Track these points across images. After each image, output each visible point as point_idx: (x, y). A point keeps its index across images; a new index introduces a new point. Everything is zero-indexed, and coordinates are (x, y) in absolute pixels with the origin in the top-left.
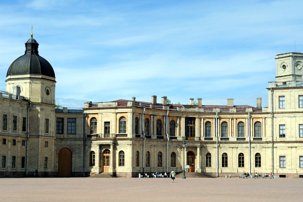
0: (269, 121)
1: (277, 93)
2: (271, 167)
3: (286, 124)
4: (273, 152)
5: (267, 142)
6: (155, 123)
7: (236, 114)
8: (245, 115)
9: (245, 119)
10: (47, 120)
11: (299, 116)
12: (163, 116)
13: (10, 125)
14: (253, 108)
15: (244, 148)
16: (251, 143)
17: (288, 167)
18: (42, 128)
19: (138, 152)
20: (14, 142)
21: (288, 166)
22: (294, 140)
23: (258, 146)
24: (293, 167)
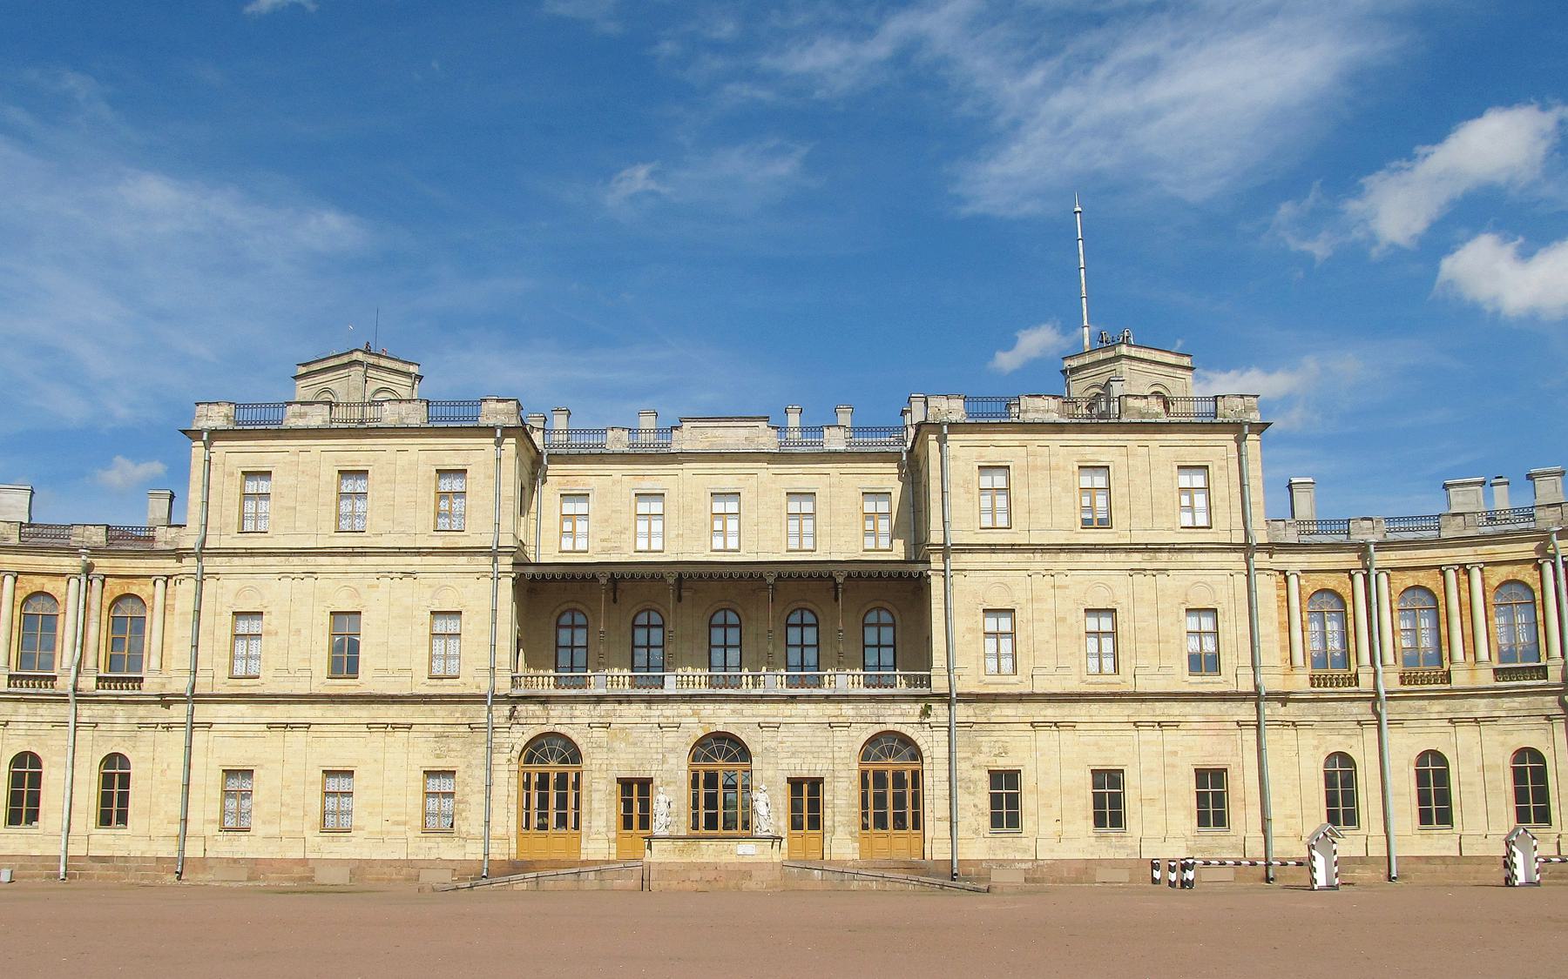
0: (184, 592)
1: (233, 457)
3: (265, 611)
5: (165, 701)
7: (16, 550)
8: (67, 561)
9: (61, 583)
11: (331, 569)
14: (108, 527)
15: (45, 726)
16: (81, 698)
17: (256, 825)
21: (264, 823)
22: (302, 689)
23: (118, 720)
24: (286, 825)
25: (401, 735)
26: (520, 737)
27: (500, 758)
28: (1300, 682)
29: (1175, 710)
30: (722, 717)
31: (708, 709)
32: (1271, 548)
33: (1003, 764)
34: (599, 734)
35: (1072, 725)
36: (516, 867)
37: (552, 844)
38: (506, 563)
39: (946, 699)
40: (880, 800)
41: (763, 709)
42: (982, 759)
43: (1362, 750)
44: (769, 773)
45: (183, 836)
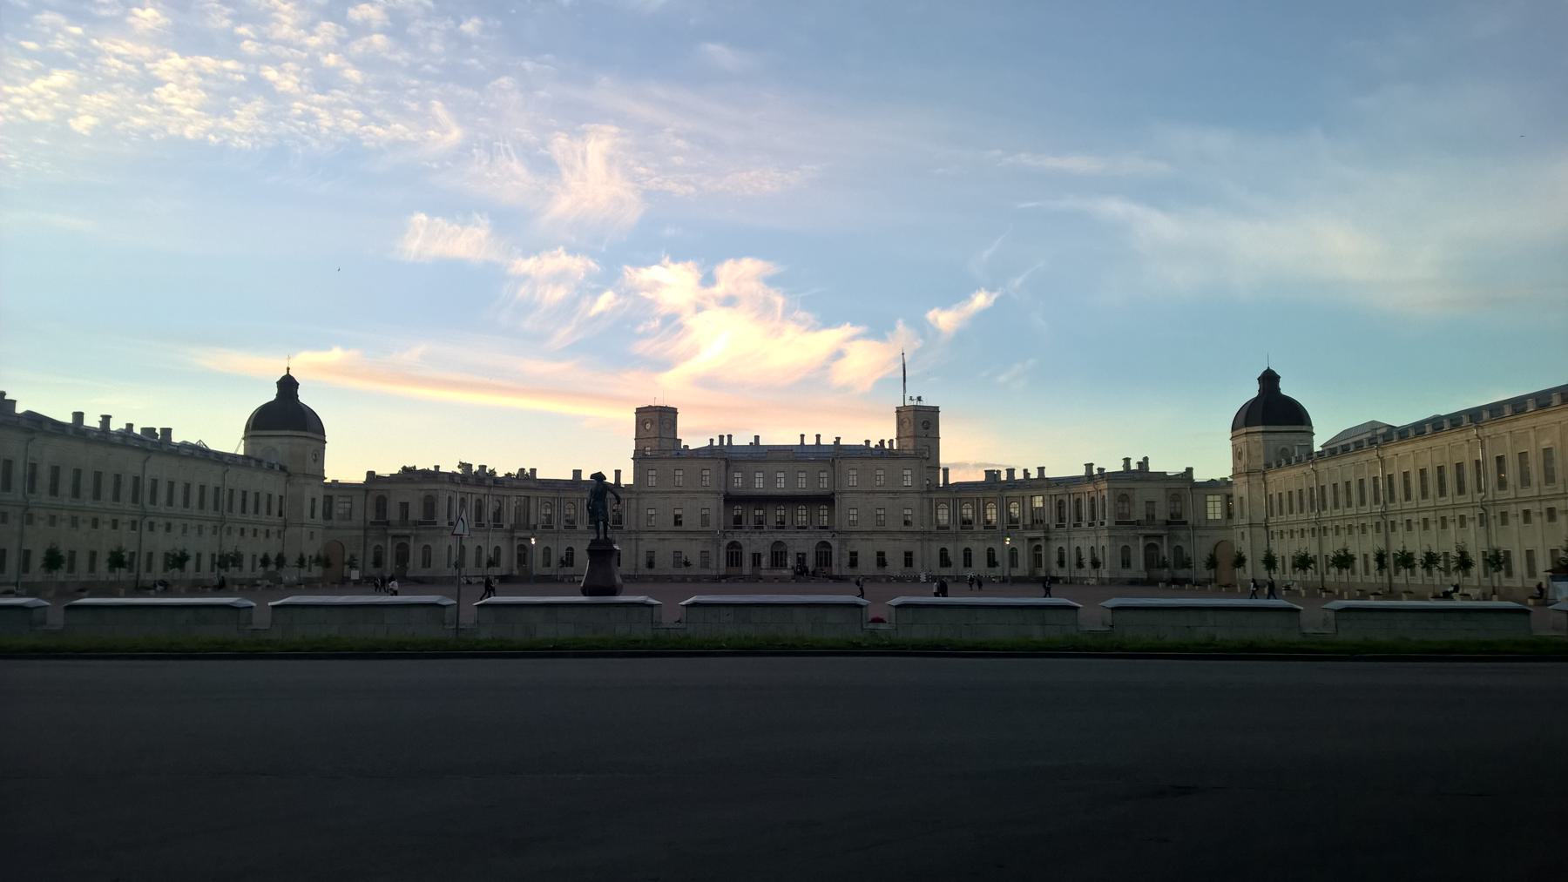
0: (634, 501)
2: (634, 567)
4: (637, 546)
6: (474, 504)
10: (313, 500)
12: (485, 495)
13: (263, 508)
18: (307, 512)
19: (450, 546)
20: (267, 534)
25: (694, 542)
26: (726, 542)
27: (721, 548)
28: (934, 528)
29: (900, 536)
30: (779, 537)
31: (775, 535)
32: (929, 491)
33: (854, 550)
34: (748, 542)
35: (872, 540)
36: (725, 577)
37: (734, 570)
38: (722, 495)
39: (838, 532)
40: (821, 559)
41: (791, 535)
42: (848, 548)
43: (950, 547)
44: (792, 552)
45: (636, 570)
